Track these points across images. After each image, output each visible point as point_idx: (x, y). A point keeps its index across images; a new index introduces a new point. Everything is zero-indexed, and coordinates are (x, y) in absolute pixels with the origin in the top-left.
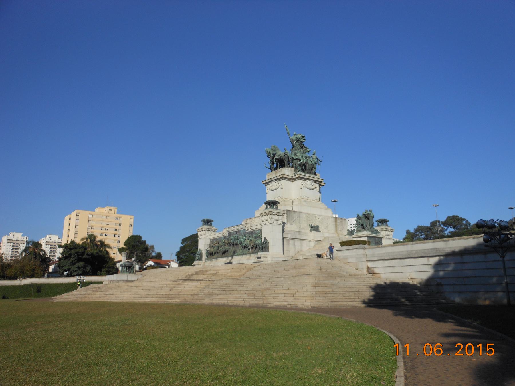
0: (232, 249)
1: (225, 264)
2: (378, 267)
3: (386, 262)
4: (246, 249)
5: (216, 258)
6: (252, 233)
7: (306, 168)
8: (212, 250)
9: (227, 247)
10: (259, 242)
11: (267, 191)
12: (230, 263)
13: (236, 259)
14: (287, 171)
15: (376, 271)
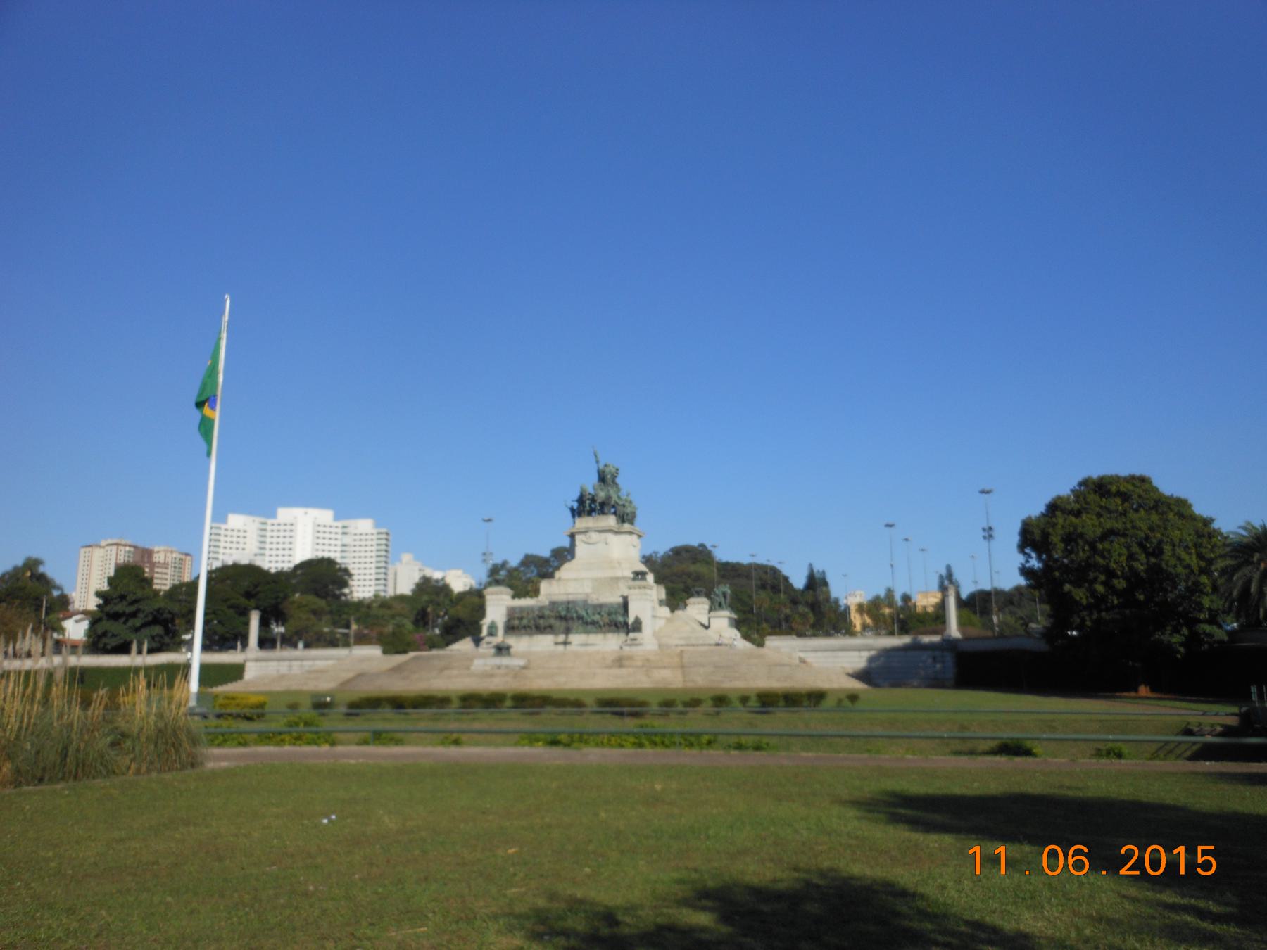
0: (557, 623)
1: (557, 644)
2: (810, 657)
3: (819, 654)
4: (590, 627)
5: (531, 634)
6: (601, 606)
7: (625, 517)
8: (516, 622)
9: (552, 621)
10: (621, 619)
11: (578, 543)
12: (565, 643)
13: (576, 639)
14: (611, 521)
15: (808, 660)
